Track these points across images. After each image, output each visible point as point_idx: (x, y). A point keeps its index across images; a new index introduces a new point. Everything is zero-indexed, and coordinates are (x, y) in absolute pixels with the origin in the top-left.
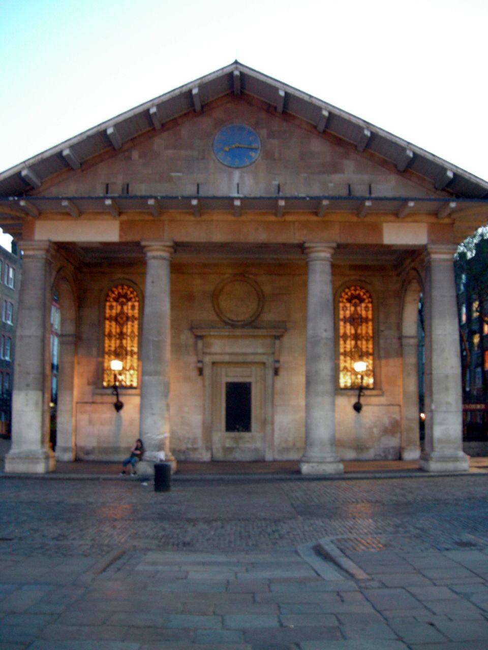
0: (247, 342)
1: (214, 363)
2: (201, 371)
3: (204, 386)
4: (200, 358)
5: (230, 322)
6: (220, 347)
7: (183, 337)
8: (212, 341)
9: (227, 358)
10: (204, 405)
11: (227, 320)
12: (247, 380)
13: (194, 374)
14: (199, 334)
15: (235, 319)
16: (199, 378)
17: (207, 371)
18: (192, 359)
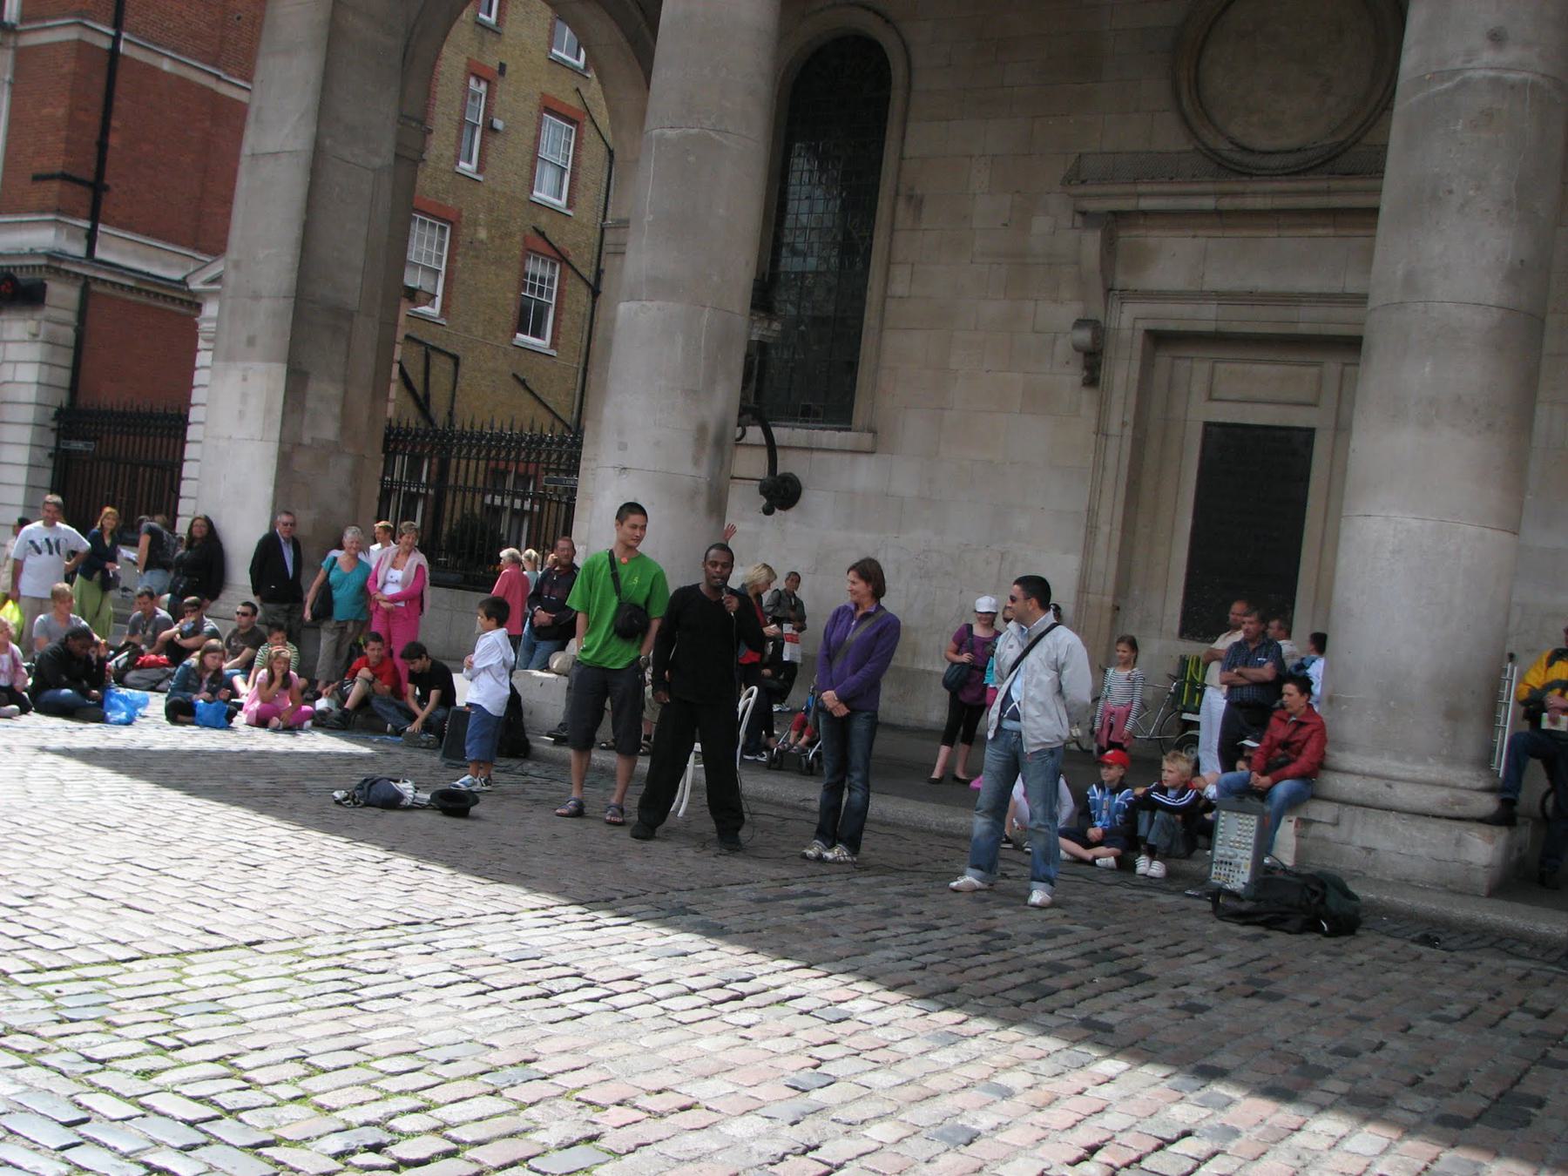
0: (1290, 241)
1: (1158, 339)
2: (1092, 363)
3: (1101, 431)
4: (1096, 312)
5: (1237, 156)
6: (1184, 269)
7: (1041, 224)
8: (1154, 238)
9: (1206, 317)
10: (1092, 513)
11: (1223, 146)
12: (1298, 418)
13: (1073, 375)
14: (1092, 206)
15: (1262, 141)
16: (1087, 396)
17: (1122, 372)
18: (1061, 315)
